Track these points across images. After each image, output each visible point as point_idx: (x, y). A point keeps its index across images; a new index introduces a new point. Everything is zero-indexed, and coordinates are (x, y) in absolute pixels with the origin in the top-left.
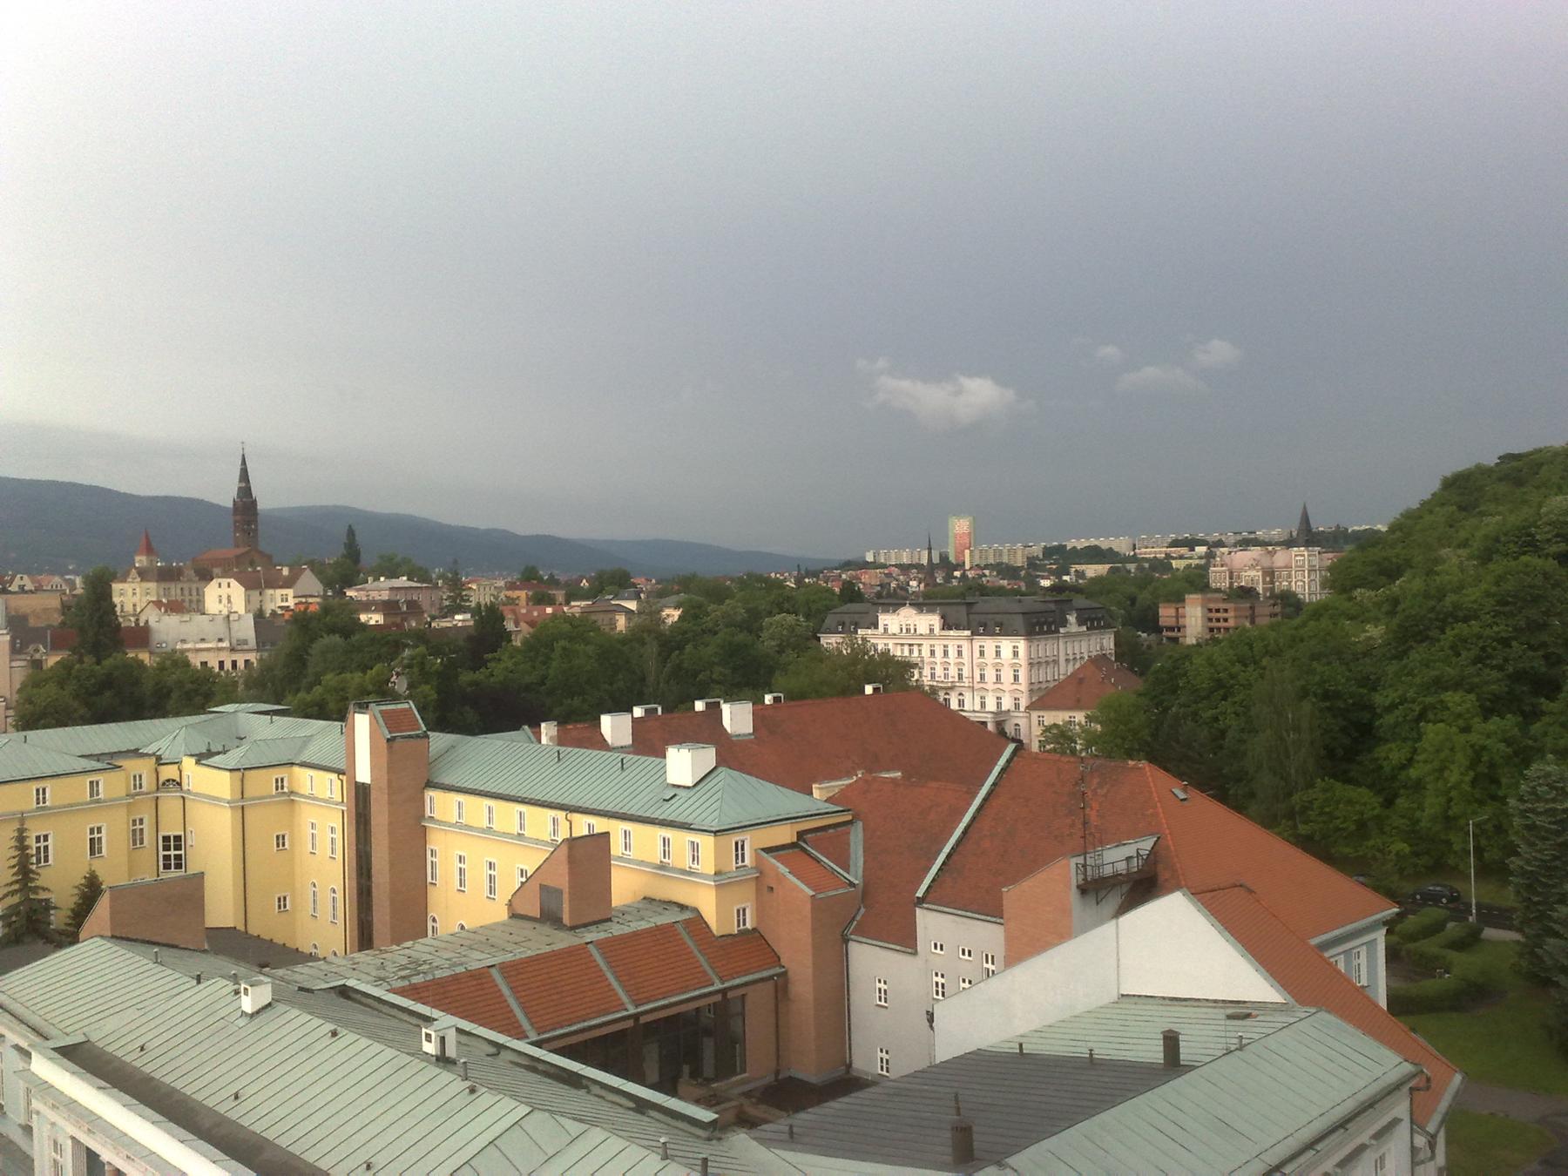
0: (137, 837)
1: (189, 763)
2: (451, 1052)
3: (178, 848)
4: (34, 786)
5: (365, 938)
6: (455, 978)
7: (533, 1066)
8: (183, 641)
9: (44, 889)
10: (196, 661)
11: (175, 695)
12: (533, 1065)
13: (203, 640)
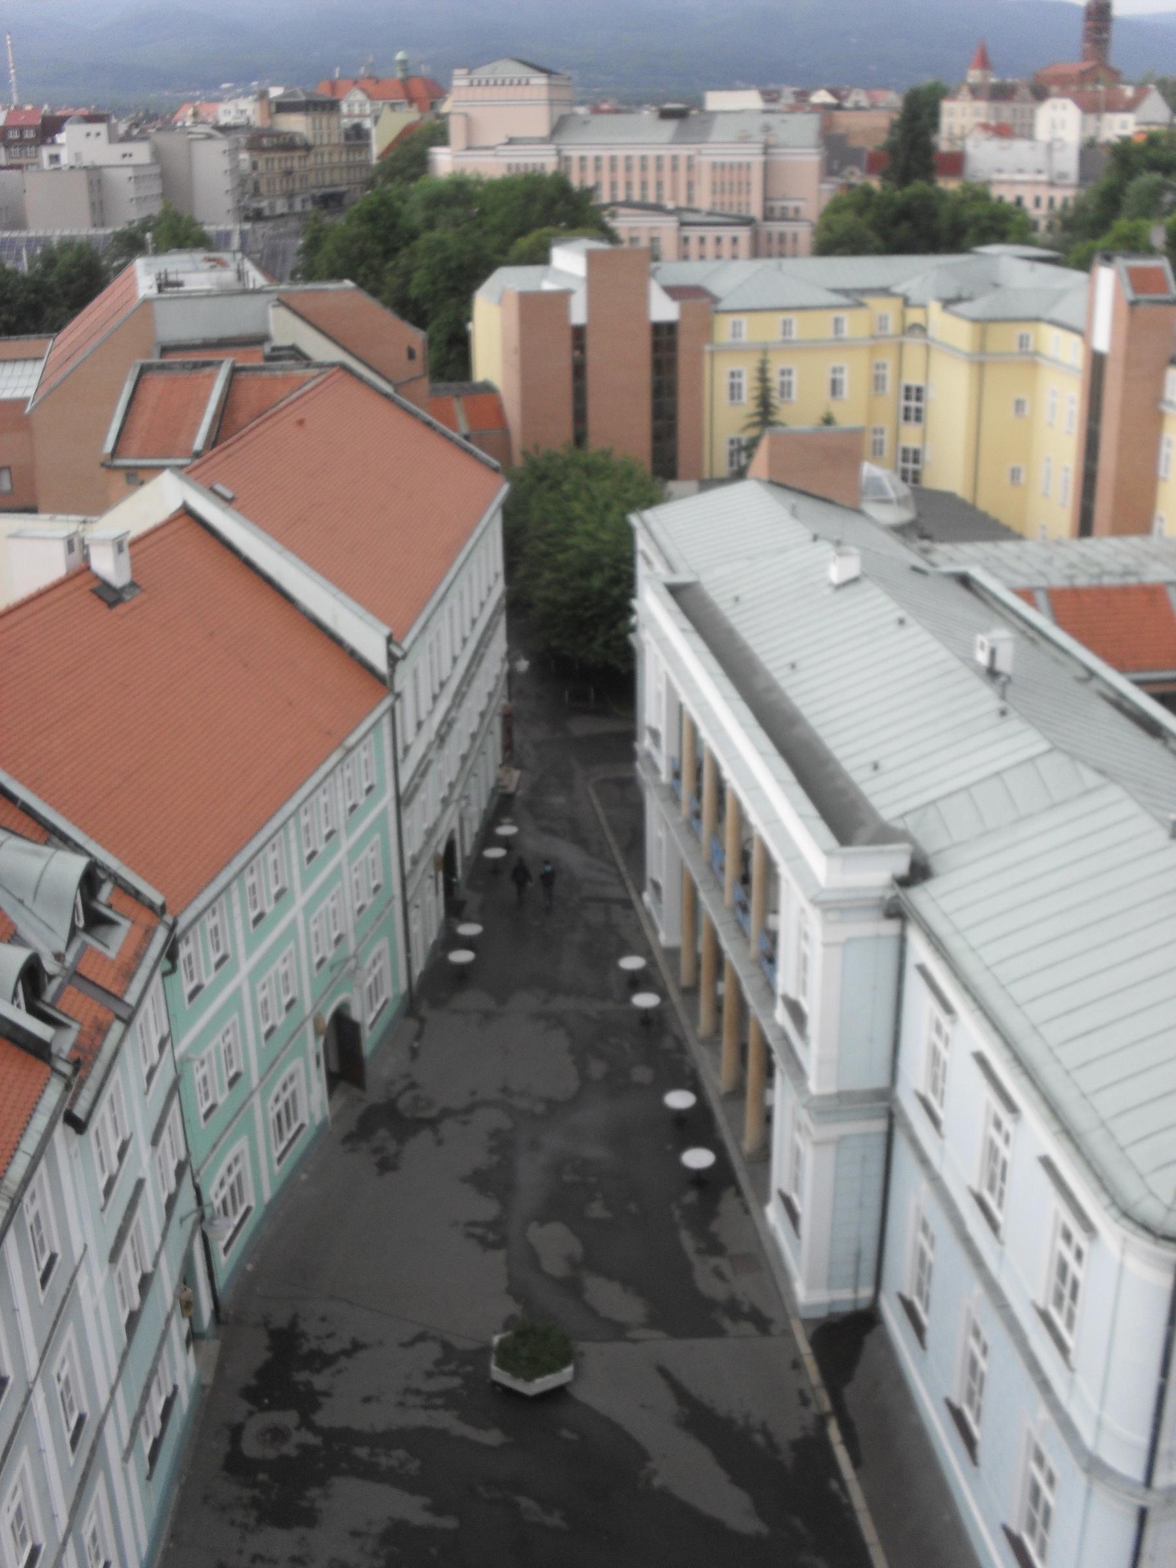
0: (878, 382)
1: (935, 308)
2: (1004, 664)
3: (918, 399)
4: (782, 317)
5: (1085, 526)
6: (1125, 590)
7: (1120, 704)
8: (1000, 171)
9: (782, 424)
10: (995, 192)
11: (972, 231)
12: (1120, 704)
13: (1021, 171)
